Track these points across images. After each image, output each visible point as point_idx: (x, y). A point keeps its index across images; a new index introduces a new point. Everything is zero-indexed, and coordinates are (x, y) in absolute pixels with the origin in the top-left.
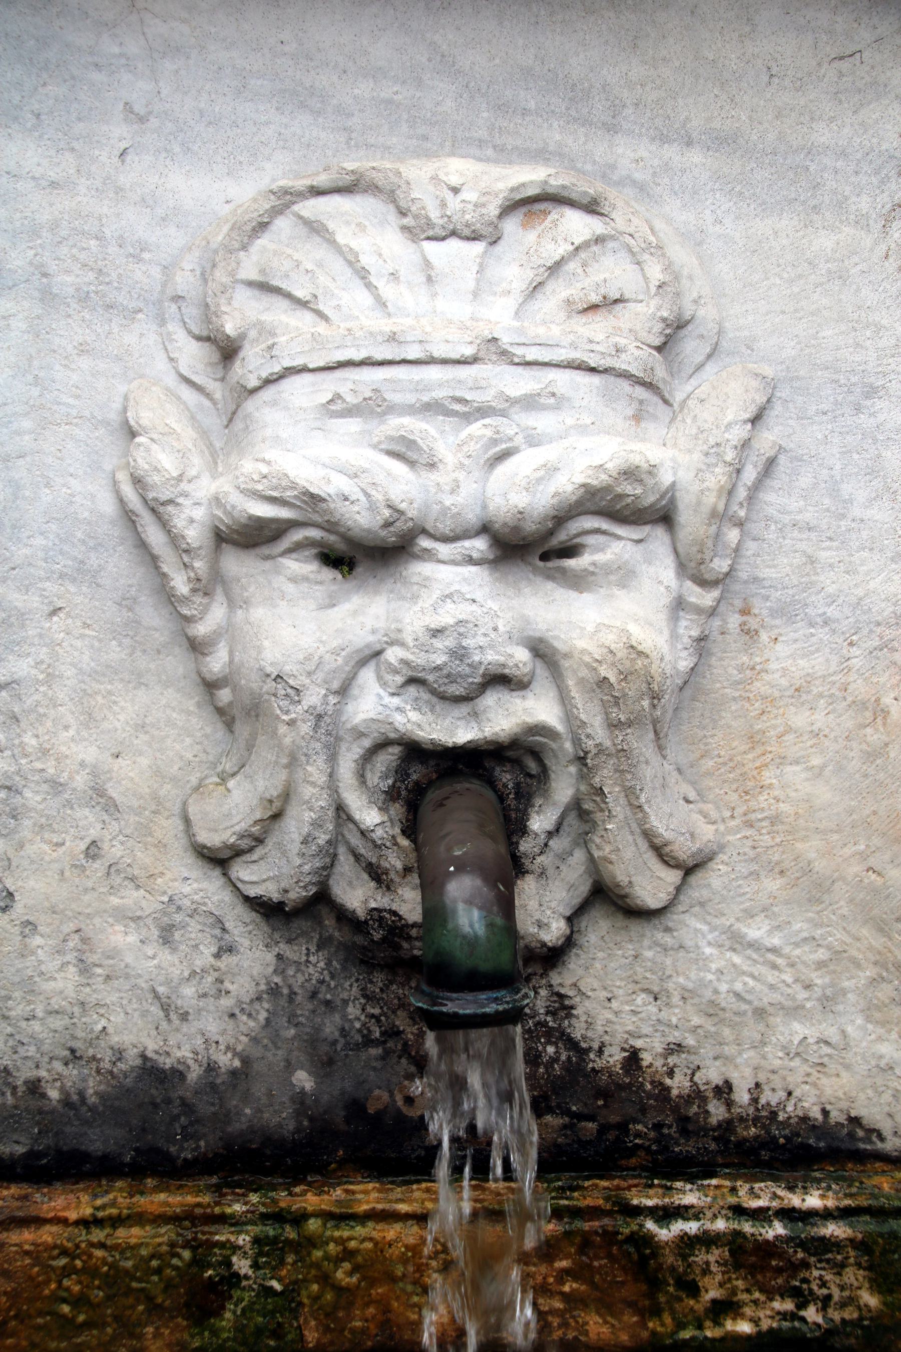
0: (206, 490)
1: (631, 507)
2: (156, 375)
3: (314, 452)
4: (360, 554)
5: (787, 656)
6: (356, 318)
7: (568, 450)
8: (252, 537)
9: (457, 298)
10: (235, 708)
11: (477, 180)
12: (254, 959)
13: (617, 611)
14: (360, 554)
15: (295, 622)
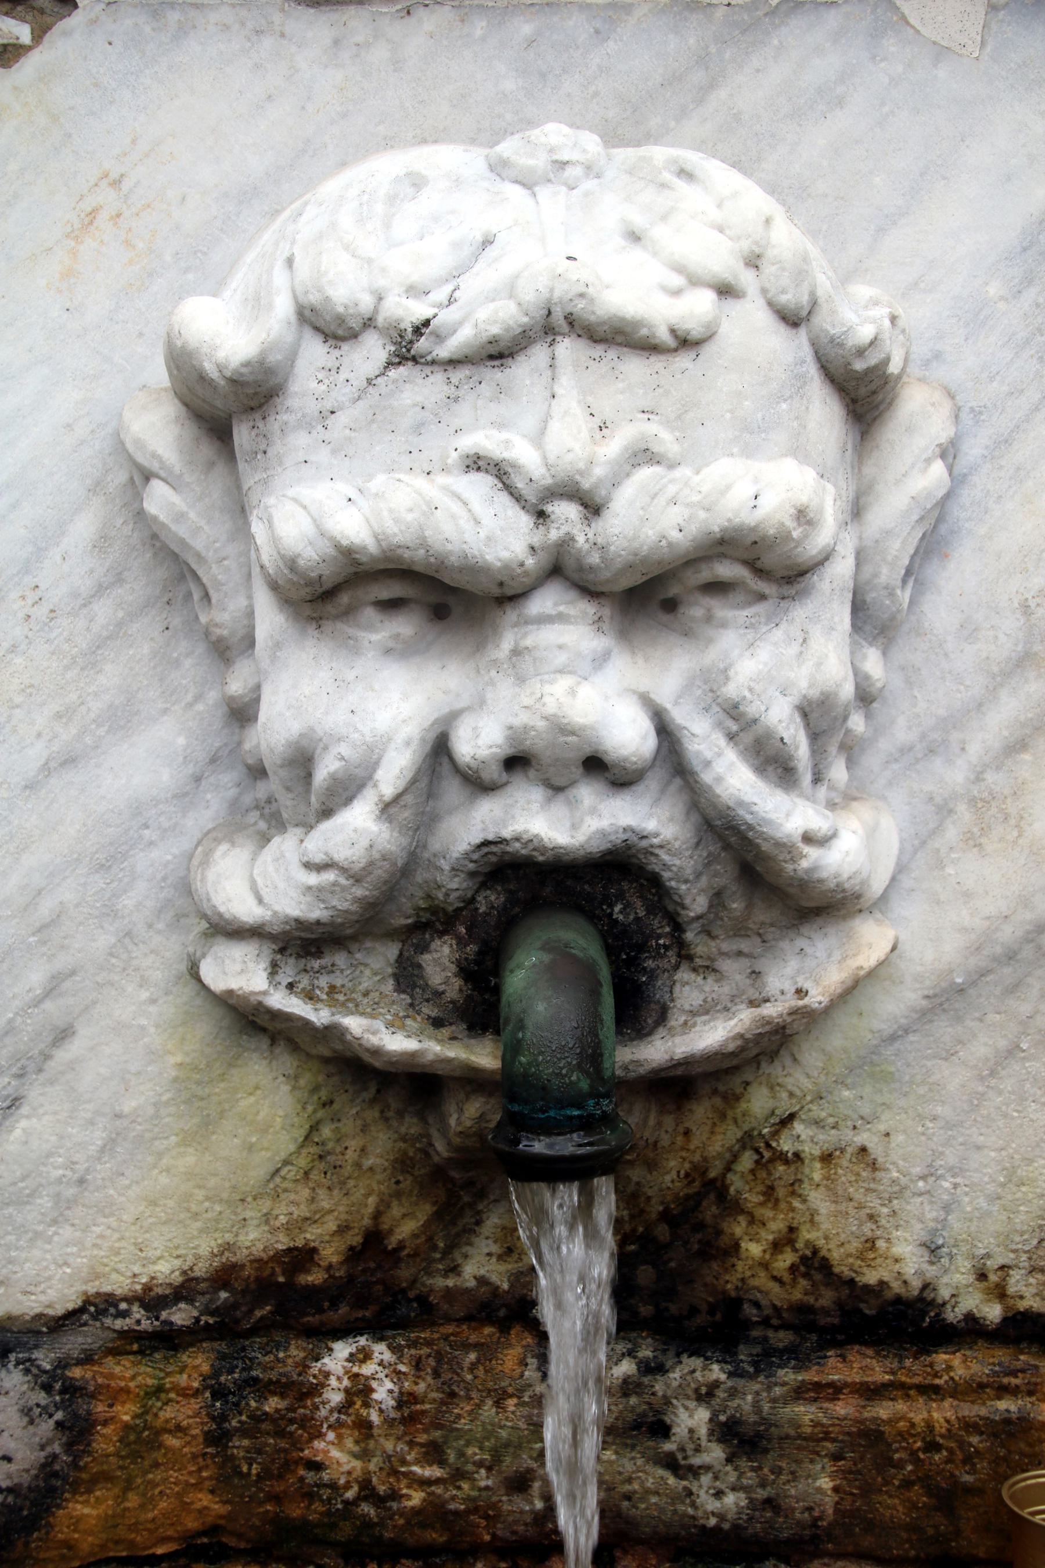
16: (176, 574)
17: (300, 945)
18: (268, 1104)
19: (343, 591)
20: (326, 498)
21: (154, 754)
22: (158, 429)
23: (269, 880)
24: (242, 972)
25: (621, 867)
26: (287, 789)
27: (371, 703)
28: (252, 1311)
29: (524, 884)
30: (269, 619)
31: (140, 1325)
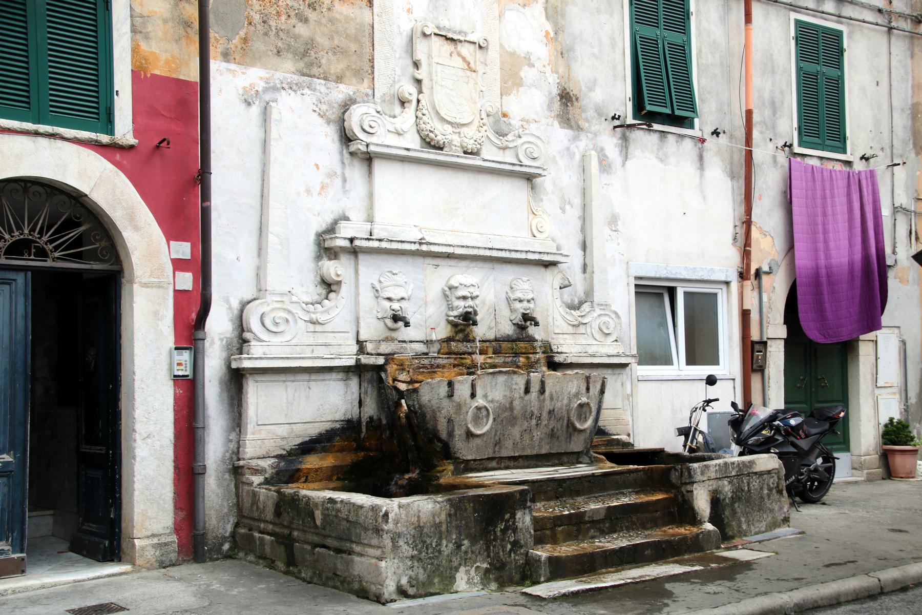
0: (512, 297)
1: (533, 299)
2: (508, 289)
3: (519, 295)
4: (521, 301)
5: (538, 309)
6: (521, 287)
7: (530, 297)
8: (515, 300)
9: (526, 286)
10: (512, 311)
11: (525, 279)
12: (513, 327)
13: (531, 305)
14: (521, 301)
15: (518, 305)
16: (446, 296)
17: (455, 317)
18: (449, 327)
19: (459, 298)
20: (461, 293)
21: (444, 307)
22: (446, 289)
23: (455, 313)
24: (451, 318)
25: (470, 313)
26: (451, 308)
27: (462, 303)
28: (449, 340)
29: (468, 313)
30: (454, 299)
31: (442, 341)
